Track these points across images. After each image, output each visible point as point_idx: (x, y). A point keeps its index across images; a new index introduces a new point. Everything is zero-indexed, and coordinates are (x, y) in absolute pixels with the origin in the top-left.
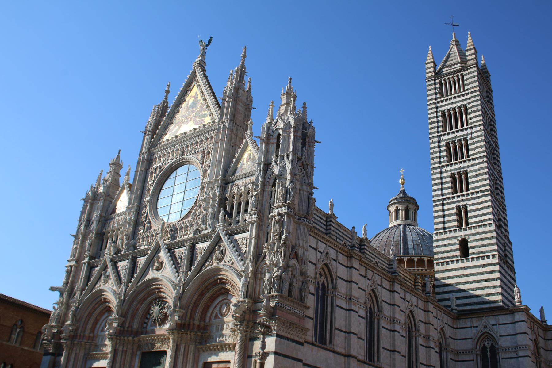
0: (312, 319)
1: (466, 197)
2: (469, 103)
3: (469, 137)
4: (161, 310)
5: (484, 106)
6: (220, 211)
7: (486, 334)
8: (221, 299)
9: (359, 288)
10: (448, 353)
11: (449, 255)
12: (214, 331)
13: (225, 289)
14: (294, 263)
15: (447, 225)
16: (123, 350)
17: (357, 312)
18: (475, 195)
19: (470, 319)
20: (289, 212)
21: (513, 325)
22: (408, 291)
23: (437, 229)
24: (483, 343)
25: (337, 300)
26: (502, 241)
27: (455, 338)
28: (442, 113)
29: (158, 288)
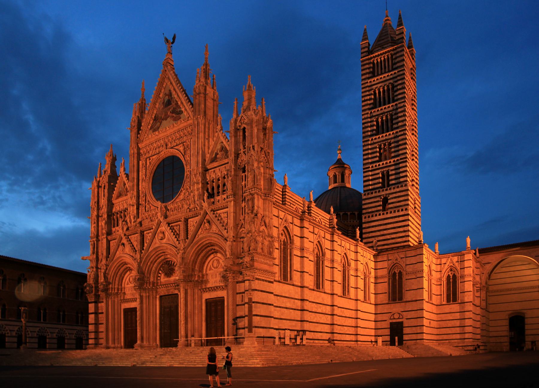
0: (278, 265)
4: (169, 267)
6: (204, 193)
8: (212, 257)
9: (309, 241)
11: (373, 210)
12: (210, 278)
13: (214, 249)
14: (263, 229)
16: (146, 296)
17: (308, 258)
20: (257, 191)
21: (415, 257)
22: (344, 240)
25: (294, 252)
29: (164, 252)
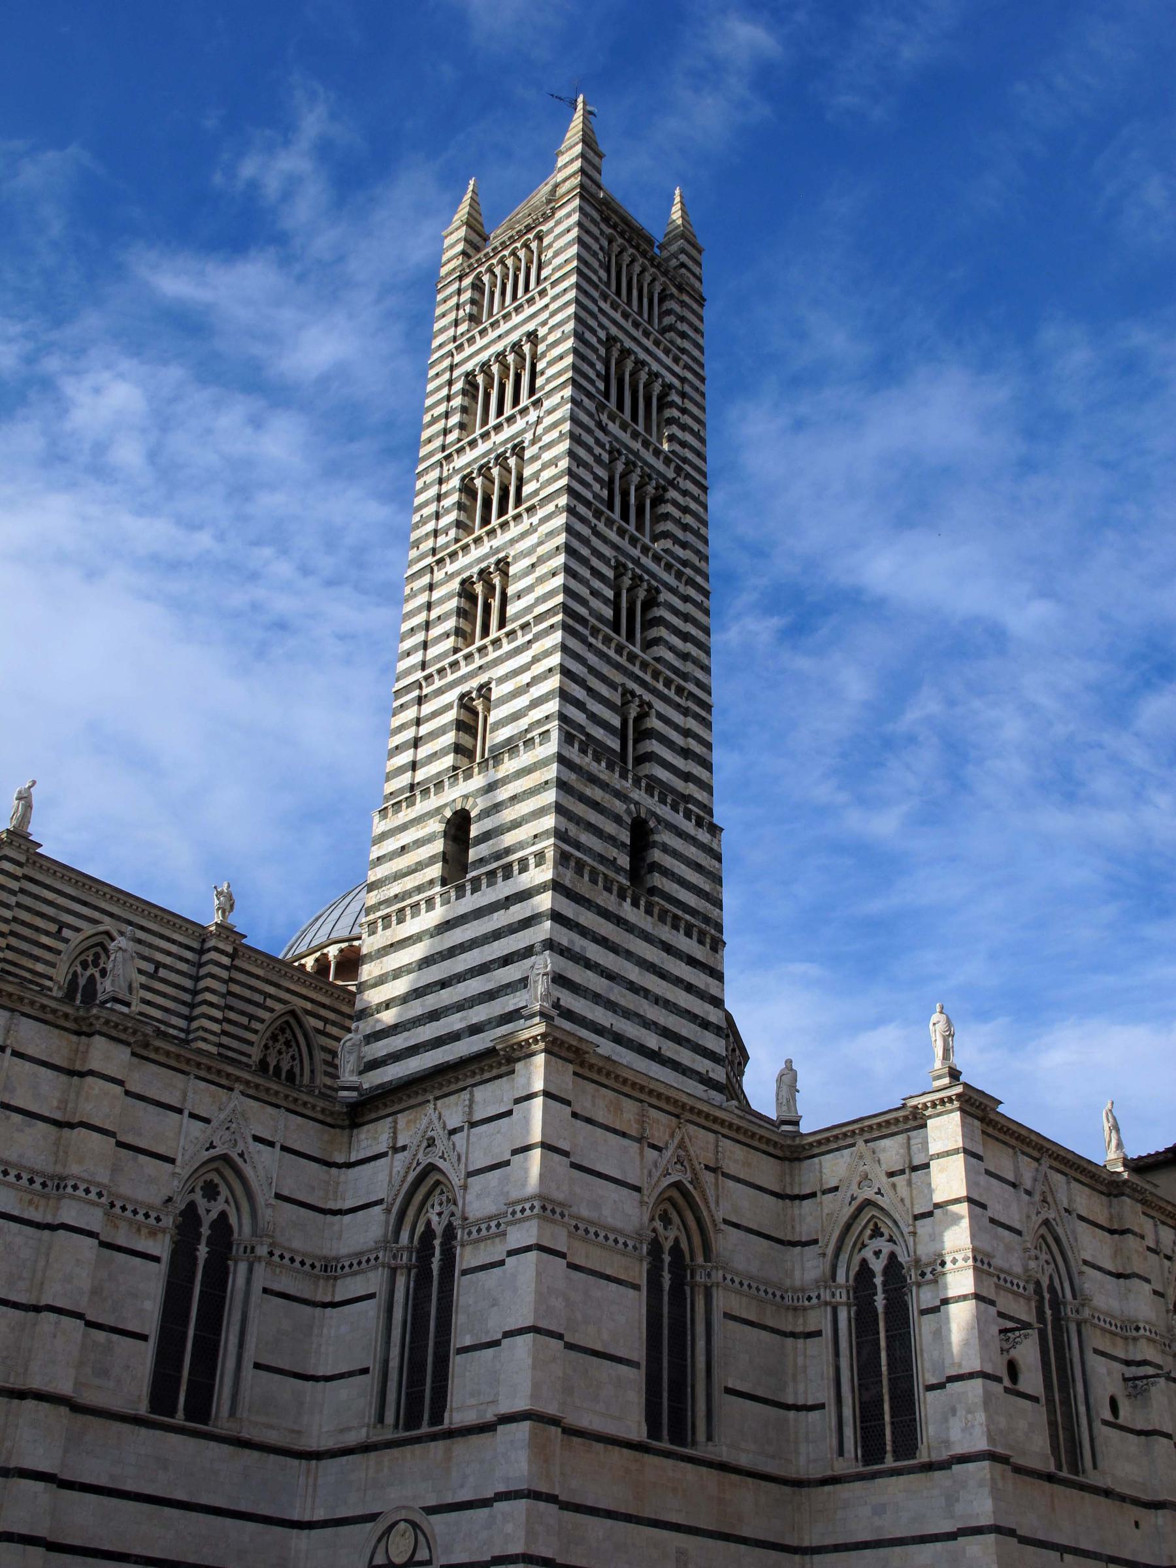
1: (492, 655)
2: (544, 323)
3: (528, 436)
5: (614, 331)
7: (435, 1177)
10: (260, 1269)
11: (409, 883)
15: (420, 775)
18: (521, 640)
19: (390, 1119)
23: (391, 794)
24: (429, 1214)
26: (619, 807)
27: (331, 1205)
28: (468, 382)
